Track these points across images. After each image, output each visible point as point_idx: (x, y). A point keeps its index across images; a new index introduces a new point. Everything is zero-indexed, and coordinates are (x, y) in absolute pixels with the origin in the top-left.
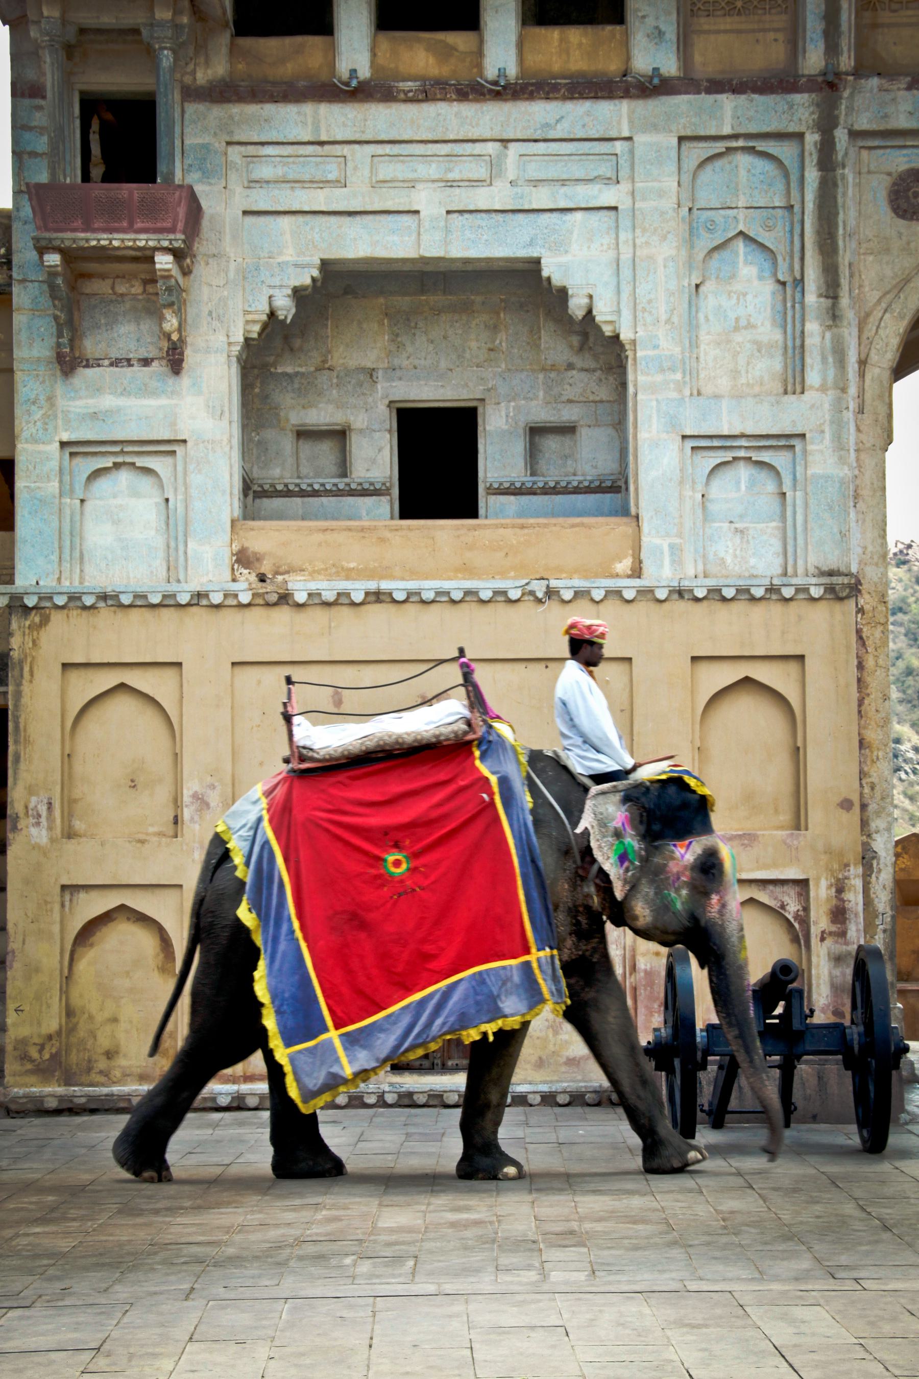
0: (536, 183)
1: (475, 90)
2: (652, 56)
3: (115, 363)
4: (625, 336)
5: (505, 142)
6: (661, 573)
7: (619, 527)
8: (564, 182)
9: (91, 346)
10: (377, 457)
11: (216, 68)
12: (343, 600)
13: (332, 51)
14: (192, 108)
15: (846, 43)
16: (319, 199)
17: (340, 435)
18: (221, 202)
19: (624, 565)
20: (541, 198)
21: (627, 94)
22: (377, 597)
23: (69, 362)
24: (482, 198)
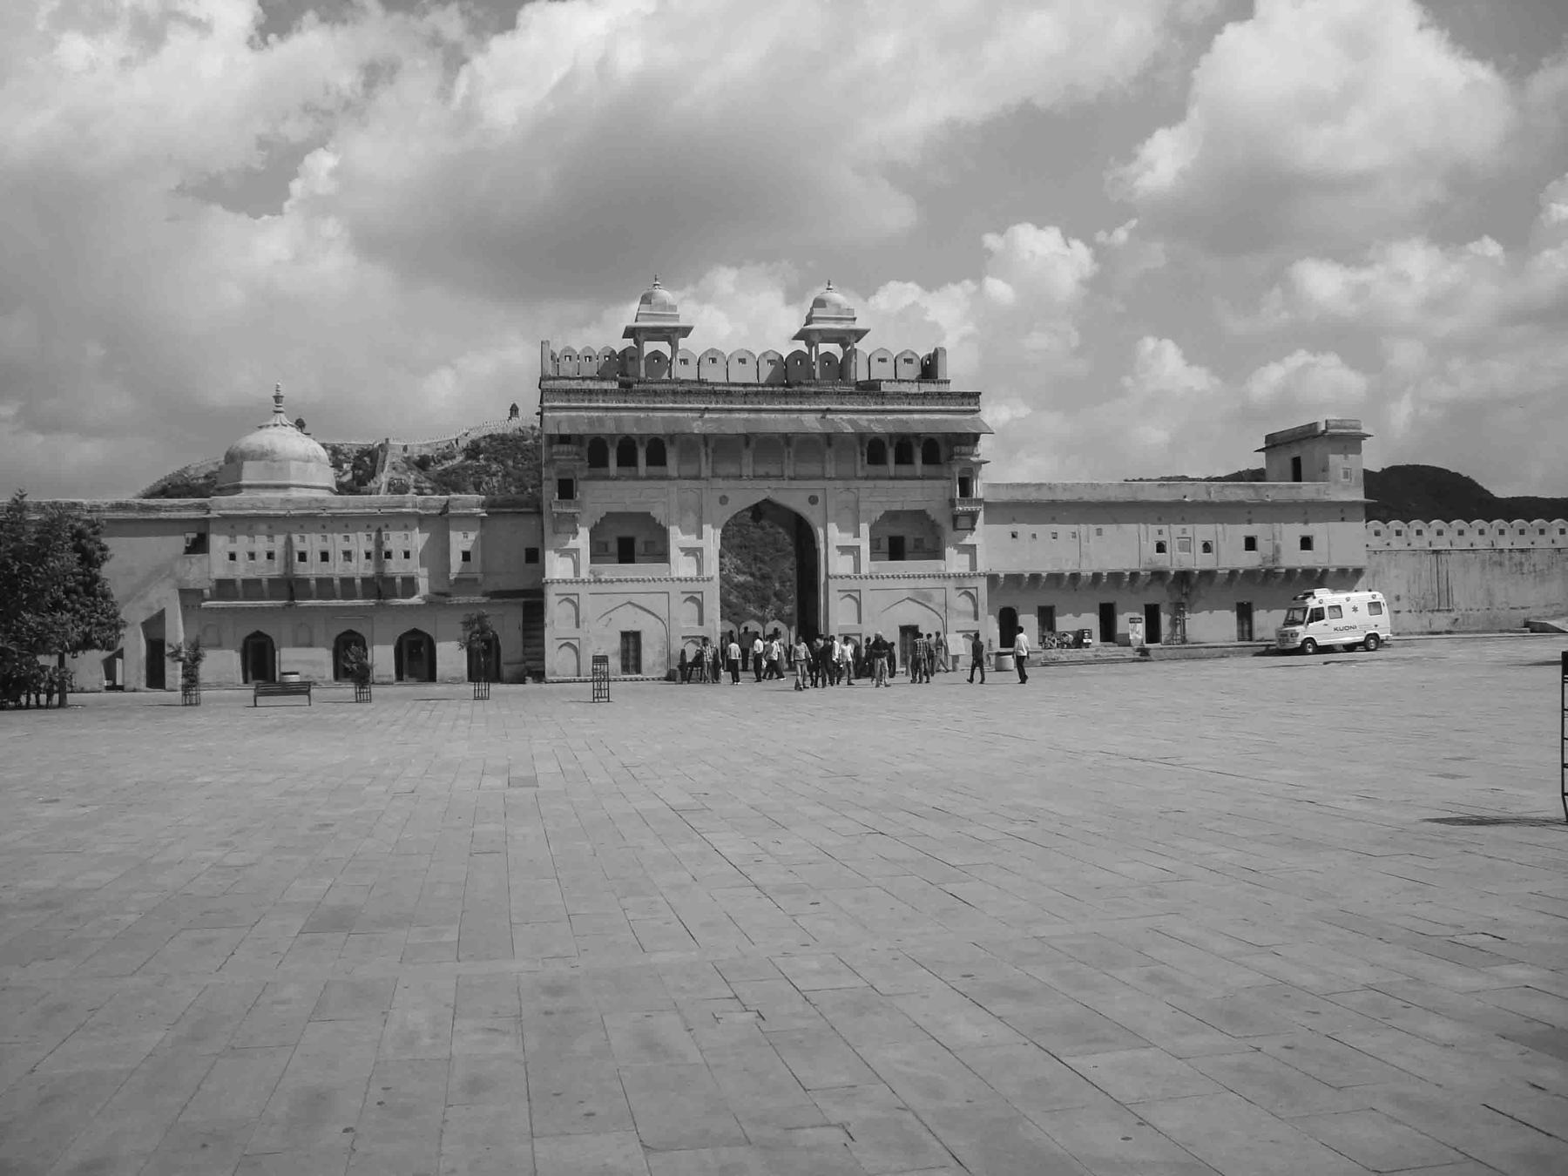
1: (637, 478)
6: (675, 575)
10: (614, 547)
11: (586, 473)
17: (606, 545)
23: (556, 532)
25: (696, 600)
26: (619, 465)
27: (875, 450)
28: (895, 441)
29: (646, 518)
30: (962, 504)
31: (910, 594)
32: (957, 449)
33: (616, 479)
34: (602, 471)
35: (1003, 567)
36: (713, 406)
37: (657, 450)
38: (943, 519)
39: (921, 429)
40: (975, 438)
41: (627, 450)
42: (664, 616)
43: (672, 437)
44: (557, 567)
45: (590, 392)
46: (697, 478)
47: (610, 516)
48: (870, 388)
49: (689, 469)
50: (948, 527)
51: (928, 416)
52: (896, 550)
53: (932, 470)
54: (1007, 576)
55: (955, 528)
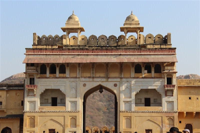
0: (59, 84)
2: (67, 76)
3: (31, 96)
4: (65, 94)
5: (58, 81)
6: (67, 110)
7: (65, 107)
8: (61, 84)
9: (30, 95)
10: (50, 101)
11: (39, 76)
12: (46, 112)
13: (46, 75)
14: (37, 79)
15: (80, 75)
16: (45, 85)
17: (48, 99)
18: (39, 85)
19: (65, 110)
20: (60, 85)
21: (66, 78)
22: (48, 112)
23: (28, 96)
24: (56, 85)
25: (74, 119)
26: (50, 73)
27: (138, 68)
28: (145, 65)
29: (58, 91)
30: (167, 87)
31: (149, 118)
32: (166, 68)
33: (48, 78)
34: (44, 75)
35: (185, 109)
36: (82, 53)
37: (63, 68)
38: (162, 92)
39: (152, 61)
40: (173, 64)
41: (53, 68)
42: (63, 124)
43: (68, 64)
44: (27, 107)
45: (41, 49)
46: (76, 78)
47: (47, 91)
48: (143, 47)
49: (74, 75)
50: (163, 95)
51: (156, 56)
52: (147, 103)
53: (157, 75)
54: (187, 113)
55: (166, 95)
